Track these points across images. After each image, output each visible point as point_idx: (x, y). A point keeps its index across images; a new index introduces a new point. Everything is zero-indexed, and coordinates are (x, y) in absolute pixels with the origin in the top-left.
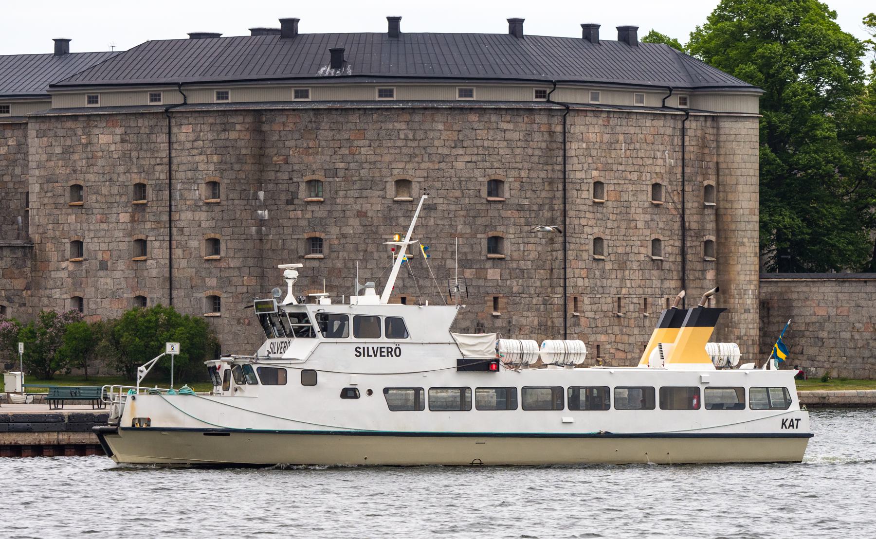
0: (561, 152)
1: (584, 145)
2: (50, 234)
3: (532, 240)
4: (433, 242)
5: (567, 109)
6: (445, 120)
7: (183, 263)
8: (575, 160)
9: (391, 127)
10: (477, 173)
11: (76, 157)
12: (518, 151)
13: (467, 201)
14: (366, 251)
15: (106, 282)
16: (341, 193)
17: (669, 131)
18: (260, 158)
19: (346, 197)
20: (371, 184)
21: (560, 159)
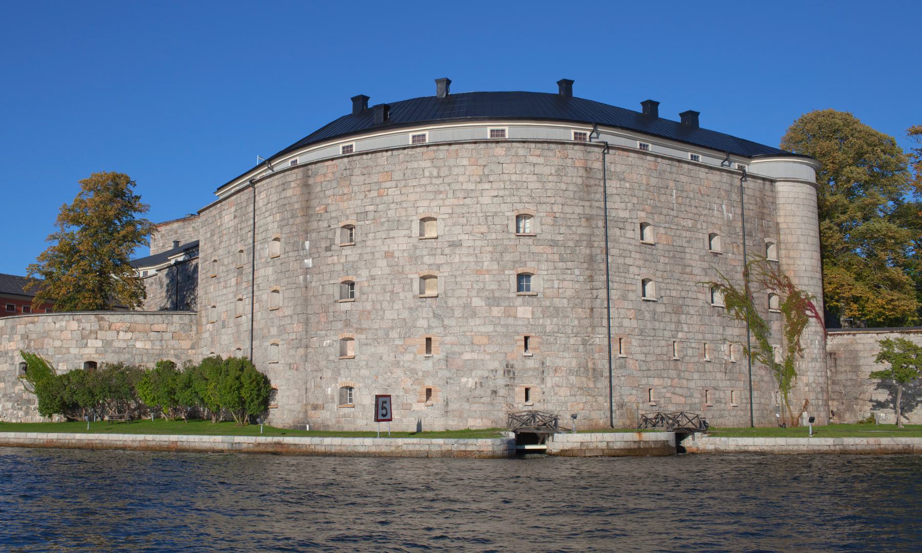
0: (602, 189)
1: (627, 185)
3: (568, 277)
4: (459, 279)
5: (607, 147)
6: (469, 155)
8: (617, 198)
9: (415, 165)
10: (504, 207)
12: (550, 185)
13: (494, 236)
14: (392, 292)
16: (371, 236)
17: (726, 187)
18: (307, 209)
19: (375, 239)
20: (398, 223)
21: (599, 196)
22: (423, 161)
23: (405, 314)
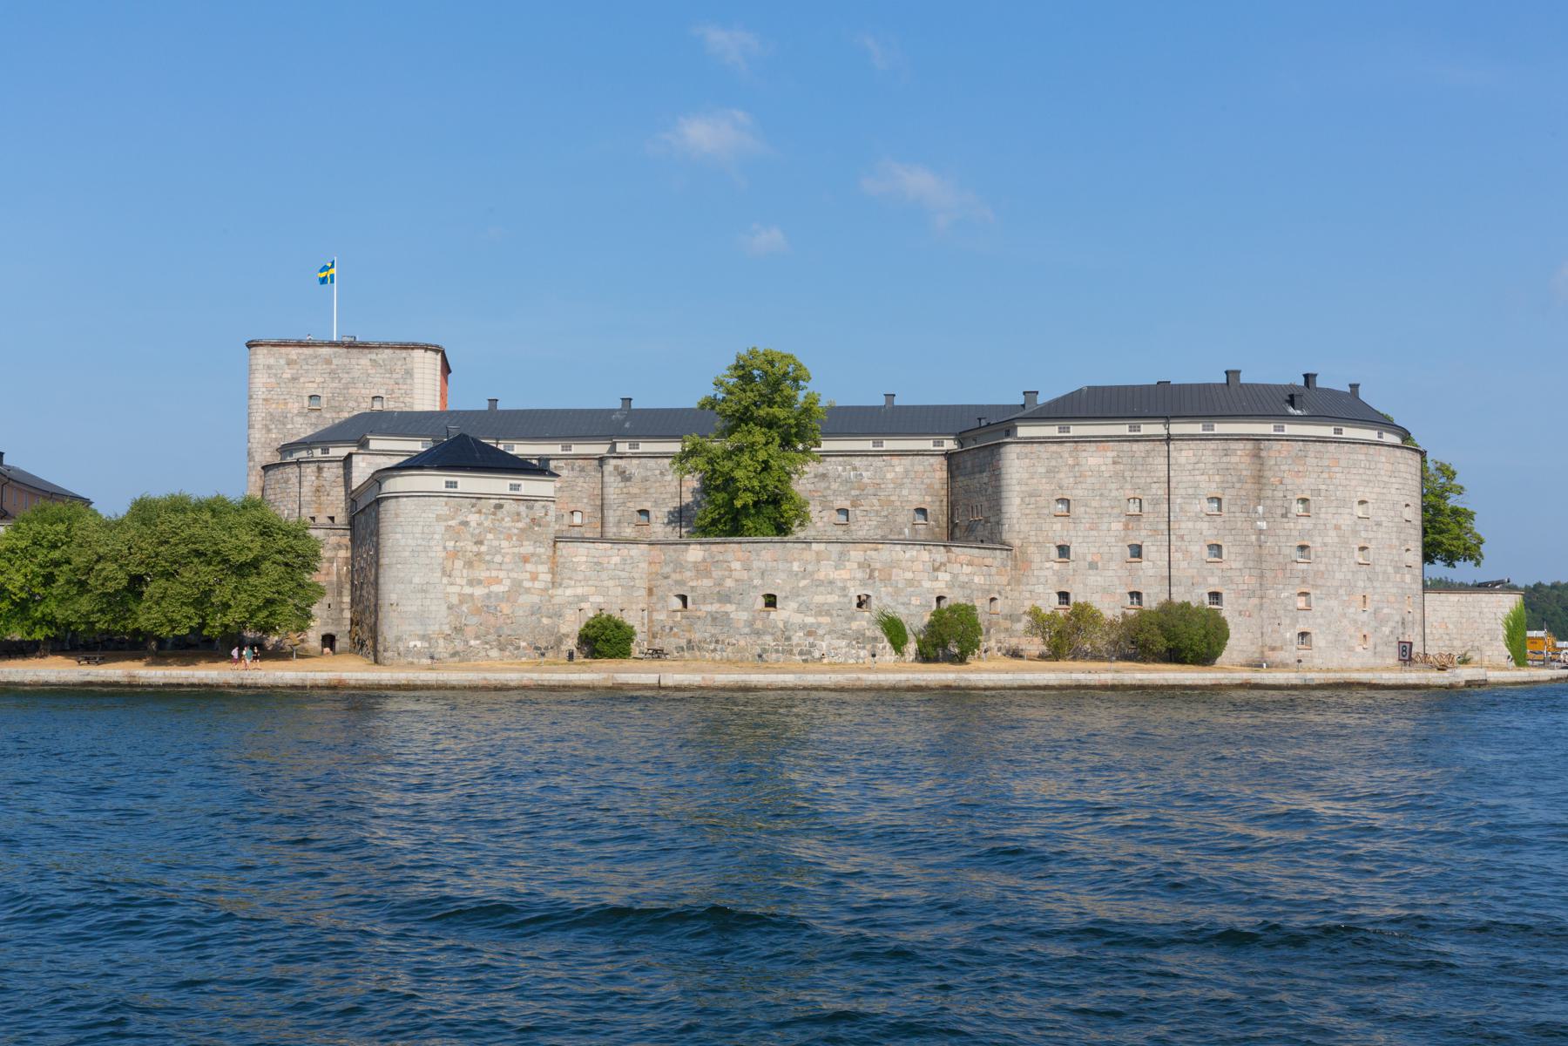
2: (1033, 539)
7: (1184, 564)
11: (1062, 475)
15: (1094, 579)
18: (1259, 478)
20: (1343, 503)
22: (1360, 454)
23: (1349, 576)
